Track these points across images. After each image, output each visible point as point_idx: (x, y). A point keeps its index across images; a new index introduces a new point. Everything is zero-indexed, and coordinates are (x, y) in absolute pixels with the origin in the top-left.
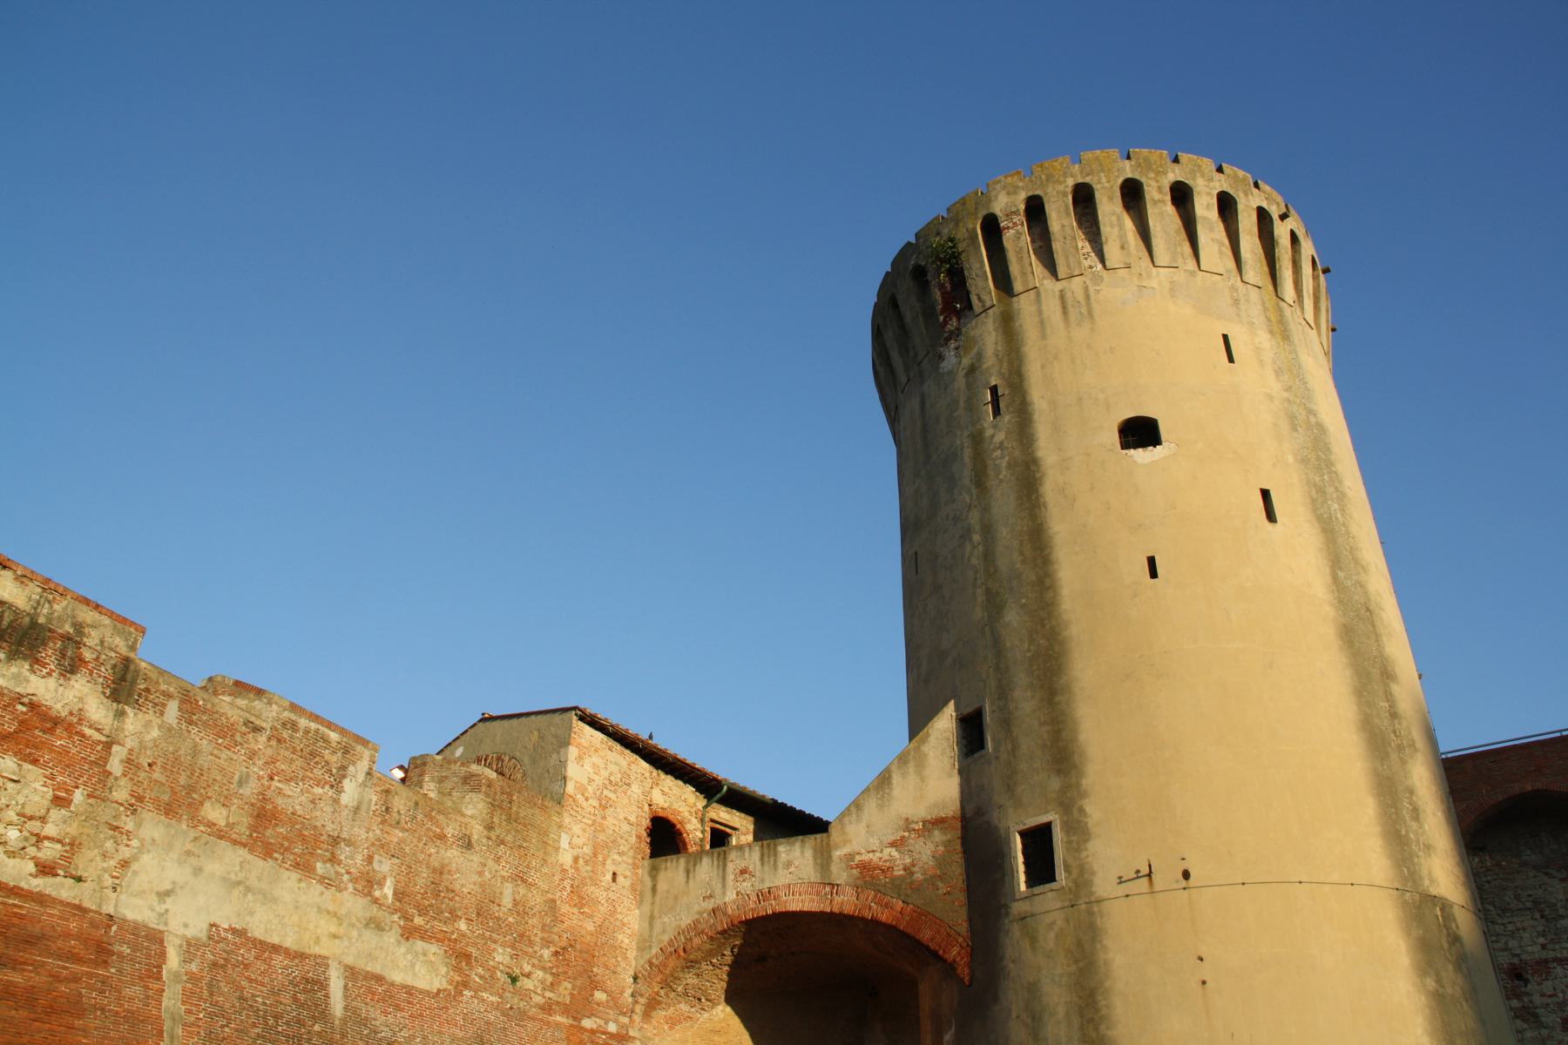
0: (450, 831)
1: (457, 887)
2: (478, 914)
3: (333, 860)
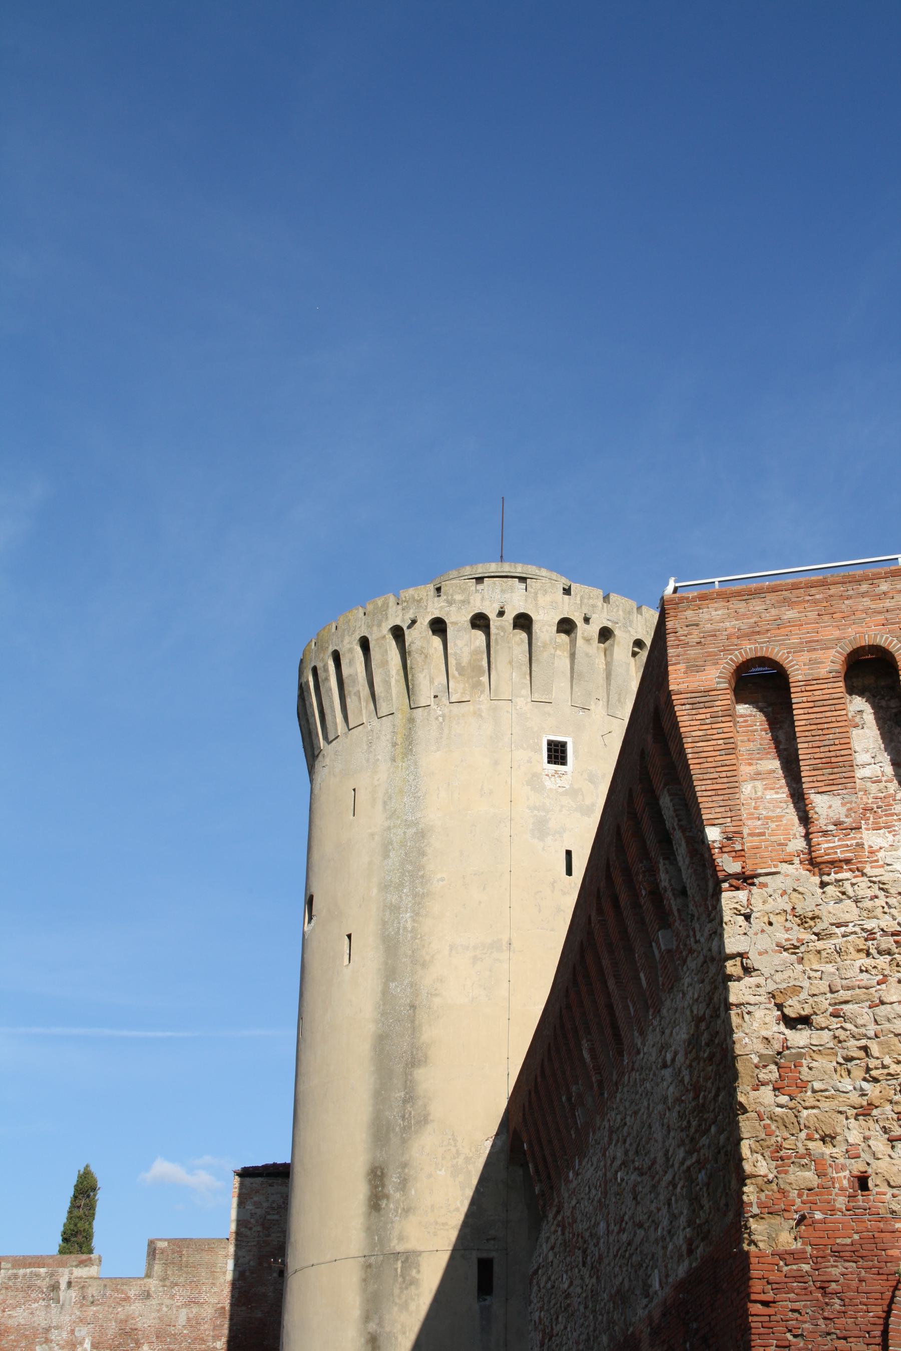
0: (132, 1293)
1: (139, 1325)
2: (157, 1337)
3: (47, 1341)
